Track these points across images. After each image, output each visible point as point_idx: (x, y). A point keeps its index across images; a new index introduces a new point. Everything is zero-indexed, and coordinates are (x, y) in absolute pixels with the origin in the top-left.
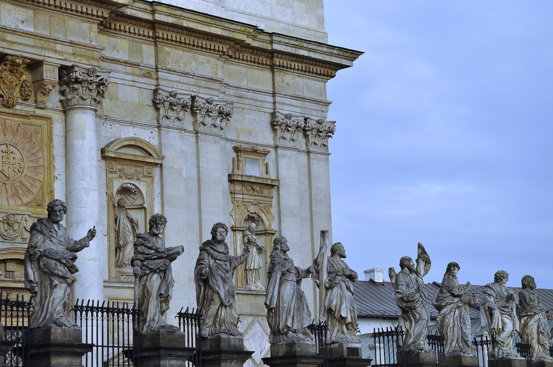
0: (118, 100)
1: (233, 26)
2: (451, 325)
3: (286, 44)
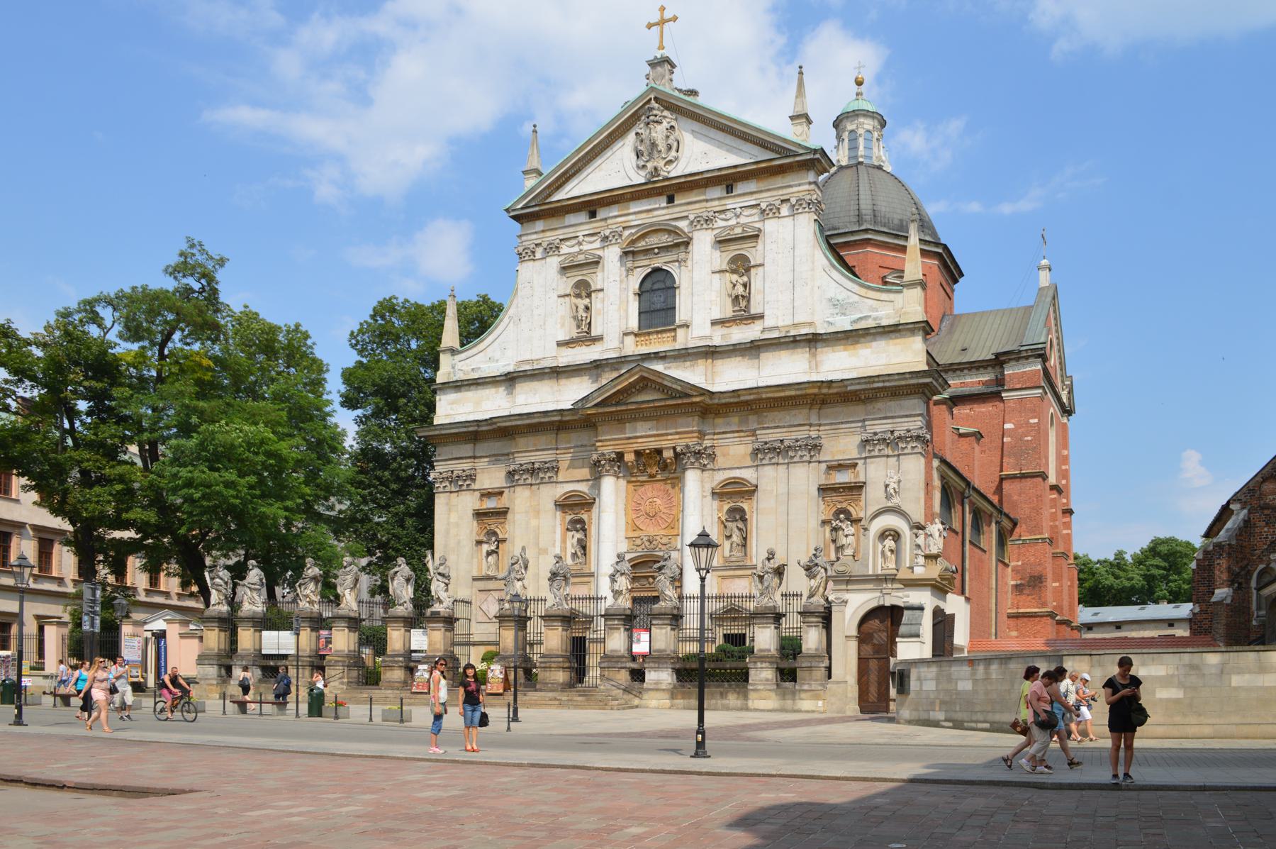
0: (728, 454)
1: (802, 386)
3: (859, 384)
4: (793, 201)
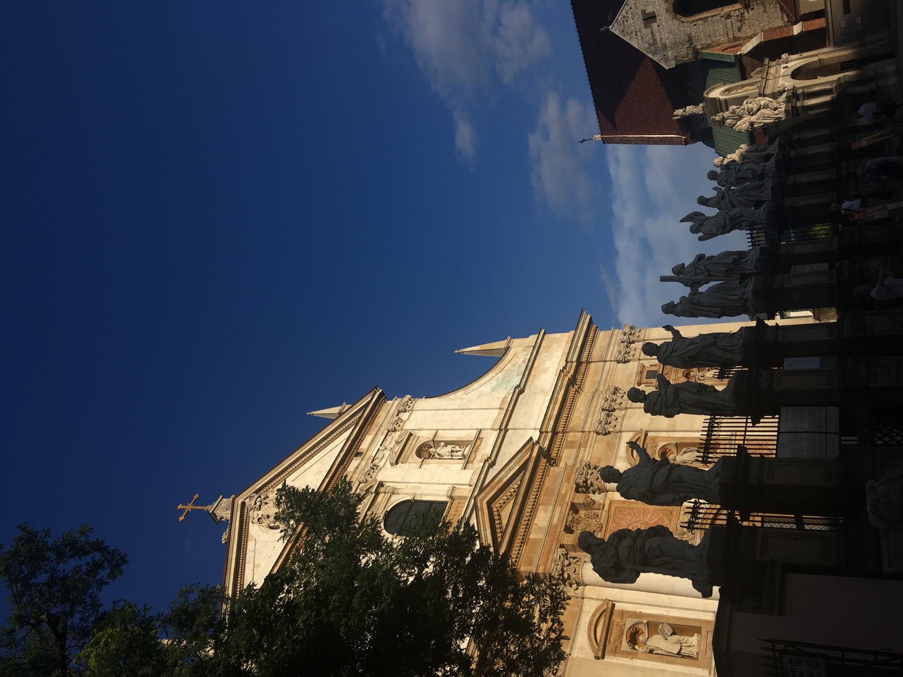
2: (747, 198)
4: (400, 409)
